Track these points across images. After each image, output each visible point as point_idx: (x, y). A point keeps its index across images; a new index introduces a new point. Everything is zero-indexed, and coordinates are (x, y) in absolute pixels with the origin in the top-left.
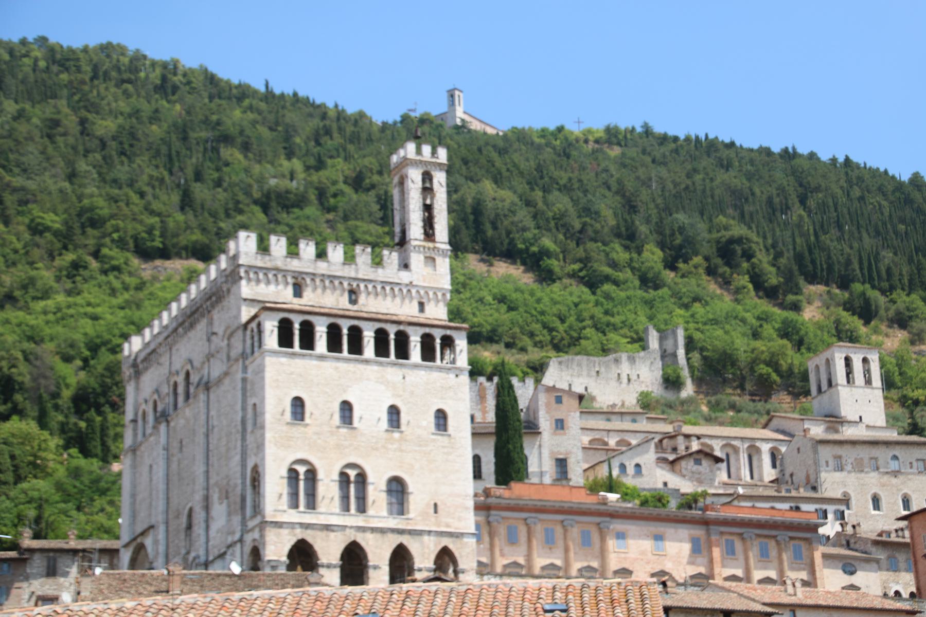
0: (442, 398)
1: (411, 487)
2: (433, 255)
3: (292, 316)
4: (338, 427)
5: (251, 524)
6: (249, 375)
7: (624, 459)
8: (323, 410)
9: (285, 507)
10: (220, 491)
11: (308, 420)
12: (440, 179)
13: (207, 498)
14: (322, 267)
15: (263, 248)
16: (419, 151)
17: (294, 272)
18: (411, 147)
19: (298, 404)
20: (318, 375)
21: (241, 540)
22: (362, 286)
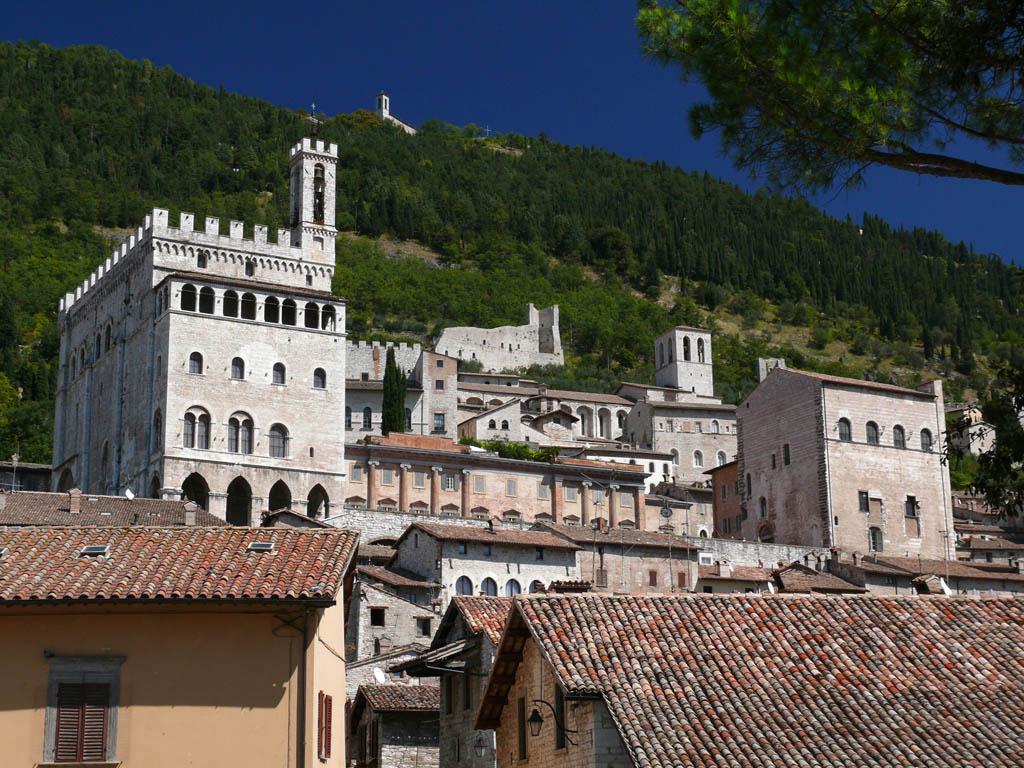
1: (291, 434)
2: (321, 236)
5: (153, 458)
6: (156, 333)
7: (494, 416)
8: (217, 363)
9: (182, 446)
10: (131, 428)
11: (204, 373)
12: (331, 169)
13: (120, 435)
14: (224, 241)
15: (174, 223)
16: (313, 146)
17: (200, 245)
18: (307, 142)
19: (197, 358)
21: (146, 471)
22: (258, 258)
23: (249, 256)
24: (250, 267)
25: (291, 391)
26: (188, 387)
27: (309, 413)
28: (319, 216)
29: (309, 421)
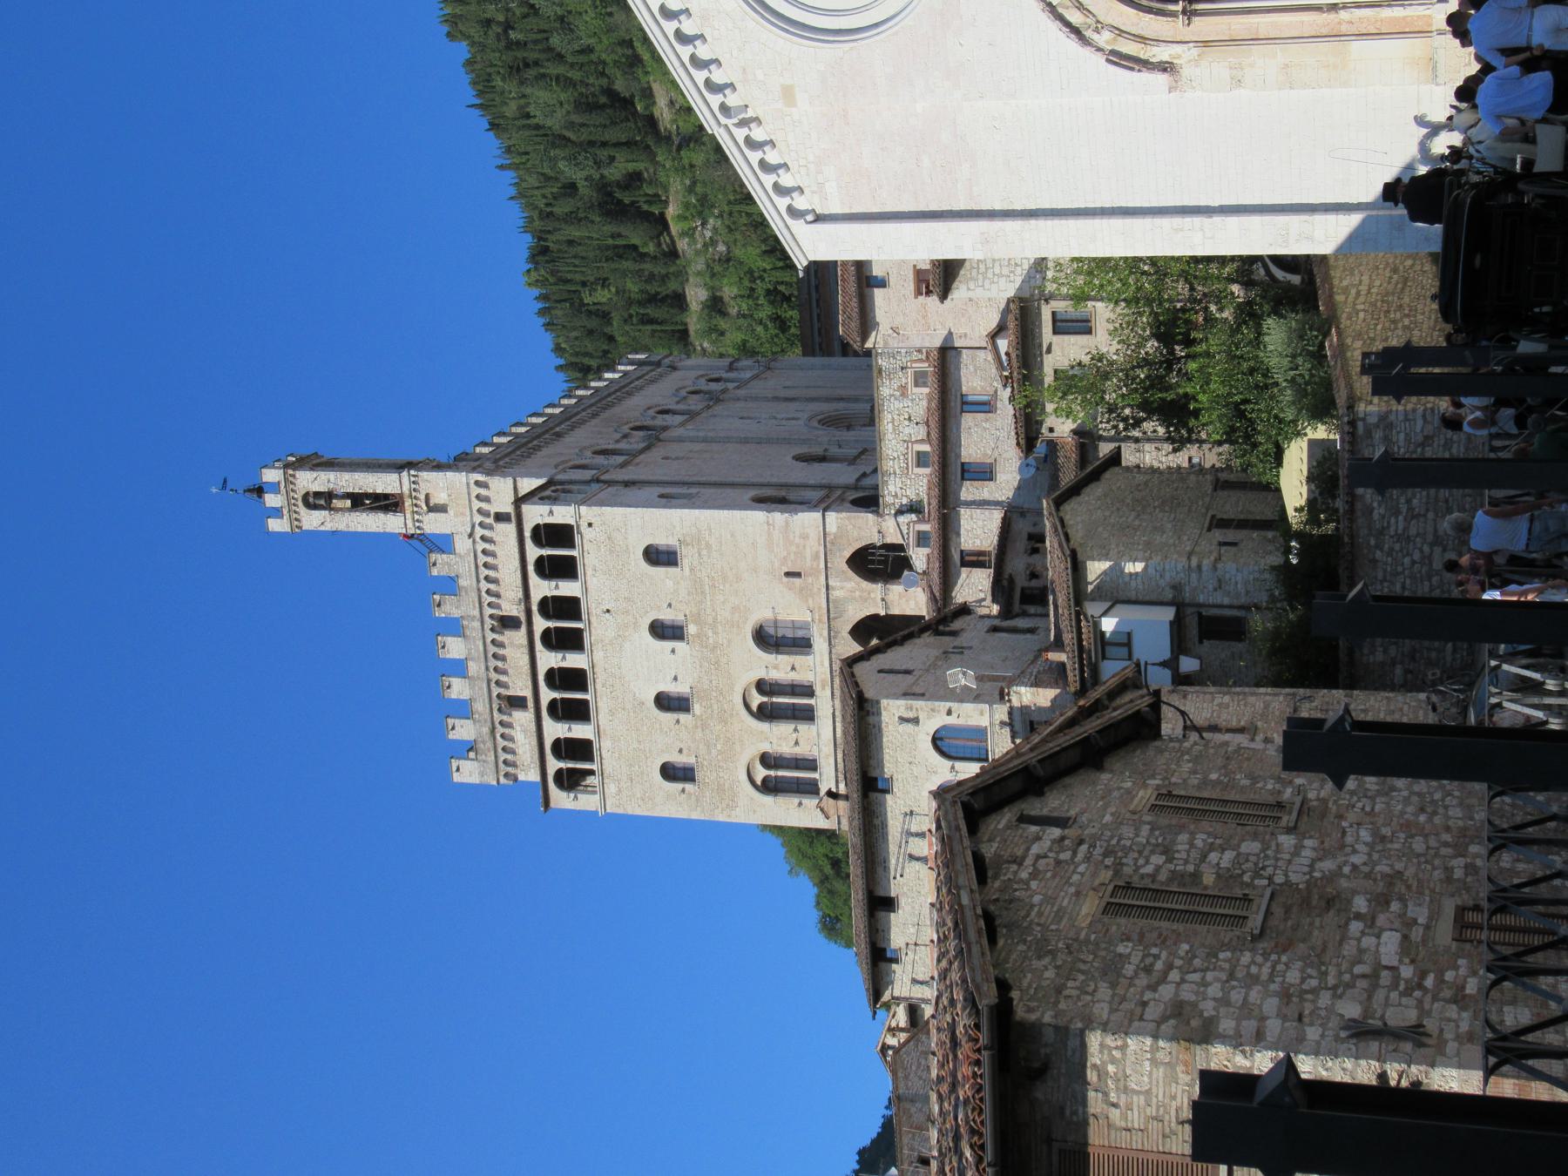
2: (422, 497)
3: (551, 772)
8: (672, 738)
12: (309, 481)
14: (474, 668)
16: (277, 513)
19: (670, 772)
20: (625, 736)
22: (488, 611)
23: (488, 626)
24: (507, 623)
25: (695, 610)
26: (721, 789)
28: (387, 503)
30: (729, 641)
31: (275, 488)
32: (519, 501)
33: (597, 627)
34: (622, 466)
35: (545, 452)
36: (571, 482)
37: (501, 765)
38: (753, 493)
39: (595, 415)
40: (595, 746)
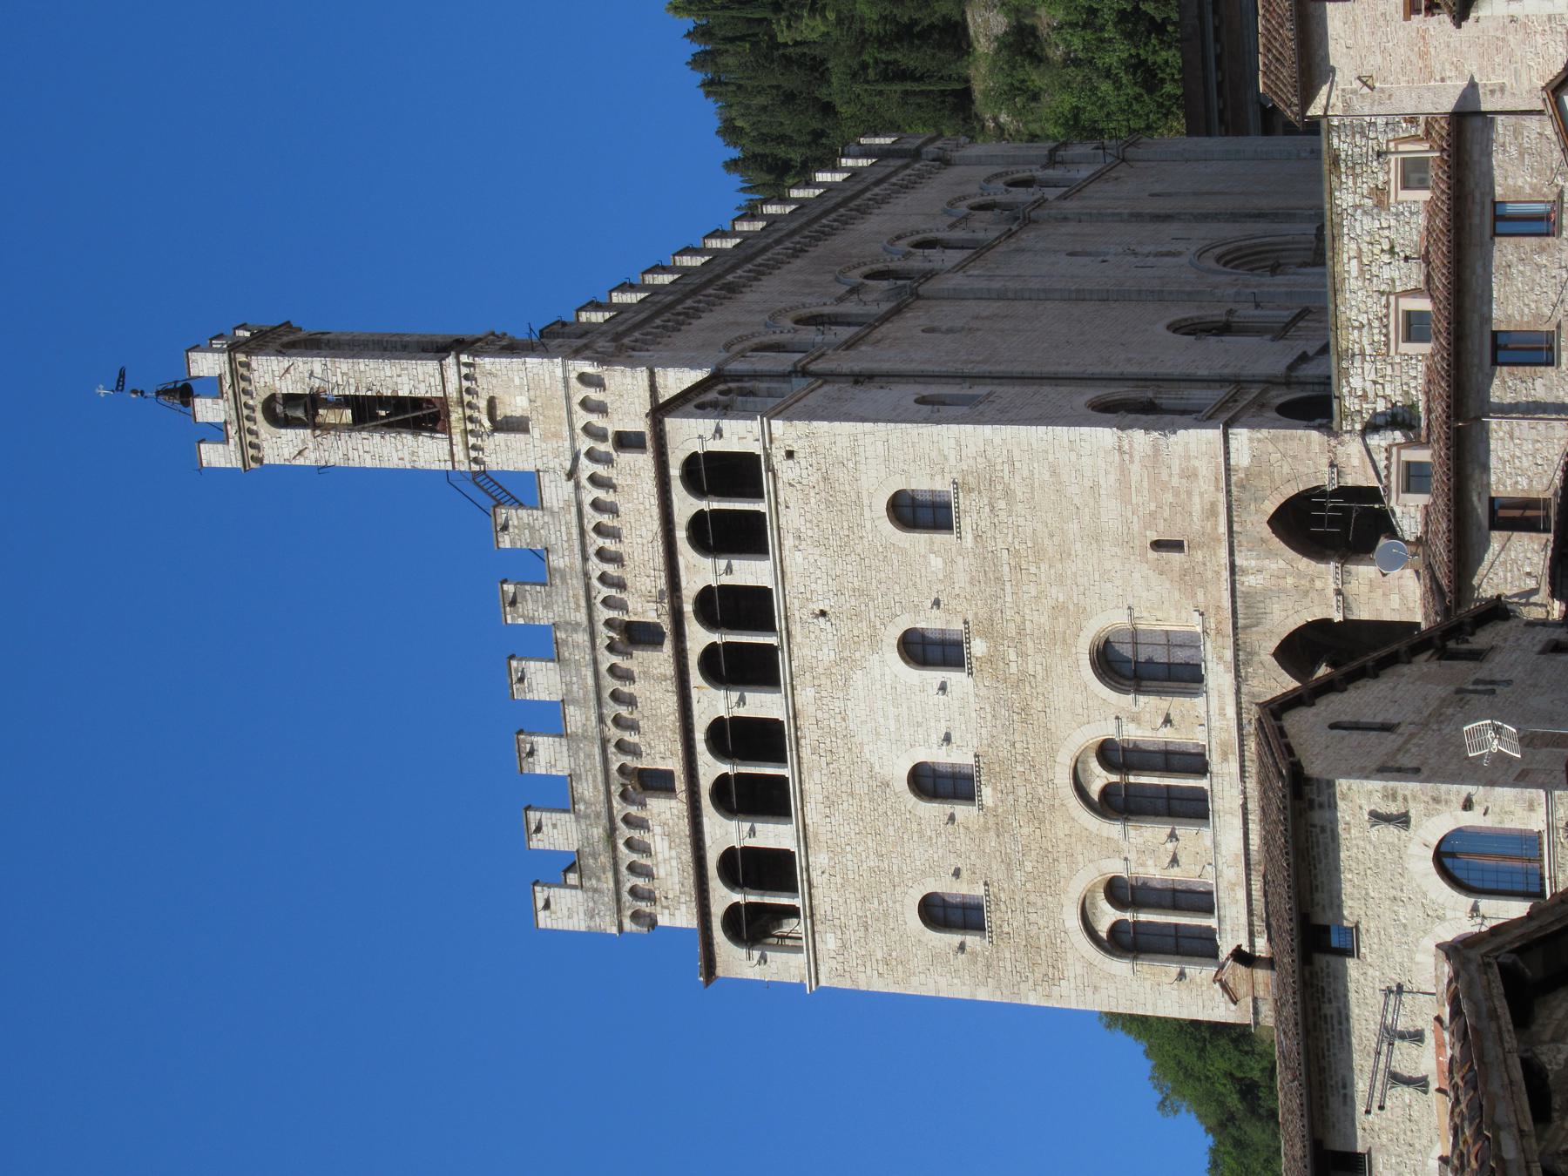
0: (858, 502)
2: (483, 404)
3: (717, 911)
4: (981, 807)
8: (939, 848)
12: (275, 374)
14: (578, 718)
16: (217, 433)
19: (941, 913)
22: (604, 614)
24: (637, 635)
25: (983, 613)
26: (1031, 946)
27: (1039, 554)
28: (421, 416)
29: (1065, 554)
30: (1047, 670)
31: (213, 387)
32: (660, 411)
33: (805, 646)
34: (849, 345)
35: (707, 319)
36: (756, 376)
37: (626, 897)
38: (1091, 393)
39: (797, 252)
40: (800, 862)
